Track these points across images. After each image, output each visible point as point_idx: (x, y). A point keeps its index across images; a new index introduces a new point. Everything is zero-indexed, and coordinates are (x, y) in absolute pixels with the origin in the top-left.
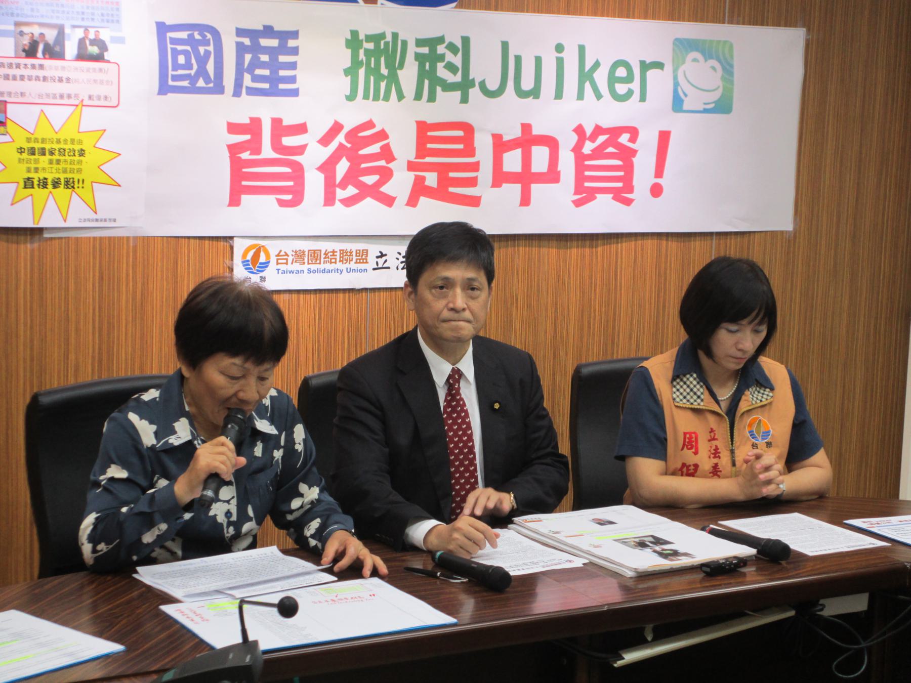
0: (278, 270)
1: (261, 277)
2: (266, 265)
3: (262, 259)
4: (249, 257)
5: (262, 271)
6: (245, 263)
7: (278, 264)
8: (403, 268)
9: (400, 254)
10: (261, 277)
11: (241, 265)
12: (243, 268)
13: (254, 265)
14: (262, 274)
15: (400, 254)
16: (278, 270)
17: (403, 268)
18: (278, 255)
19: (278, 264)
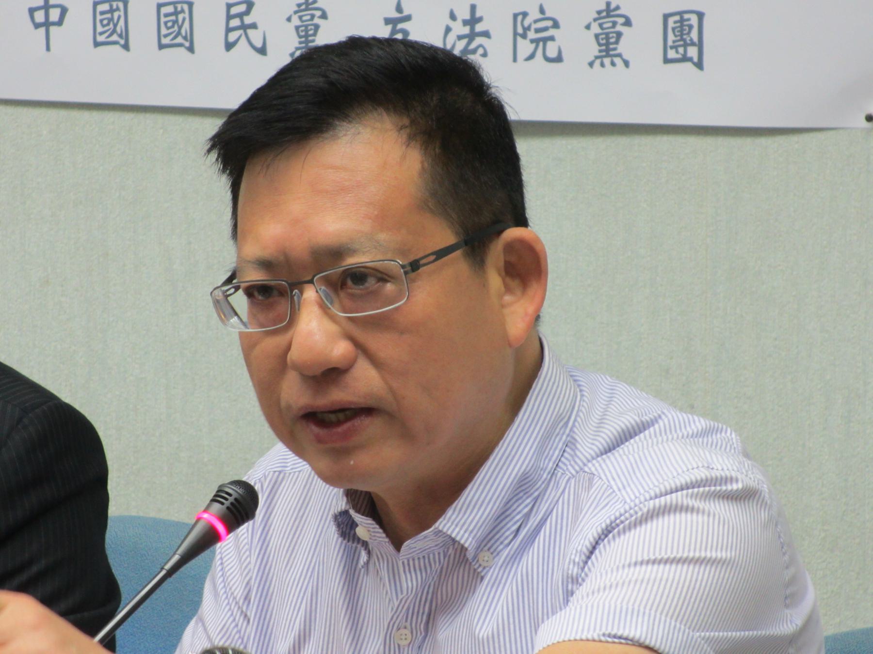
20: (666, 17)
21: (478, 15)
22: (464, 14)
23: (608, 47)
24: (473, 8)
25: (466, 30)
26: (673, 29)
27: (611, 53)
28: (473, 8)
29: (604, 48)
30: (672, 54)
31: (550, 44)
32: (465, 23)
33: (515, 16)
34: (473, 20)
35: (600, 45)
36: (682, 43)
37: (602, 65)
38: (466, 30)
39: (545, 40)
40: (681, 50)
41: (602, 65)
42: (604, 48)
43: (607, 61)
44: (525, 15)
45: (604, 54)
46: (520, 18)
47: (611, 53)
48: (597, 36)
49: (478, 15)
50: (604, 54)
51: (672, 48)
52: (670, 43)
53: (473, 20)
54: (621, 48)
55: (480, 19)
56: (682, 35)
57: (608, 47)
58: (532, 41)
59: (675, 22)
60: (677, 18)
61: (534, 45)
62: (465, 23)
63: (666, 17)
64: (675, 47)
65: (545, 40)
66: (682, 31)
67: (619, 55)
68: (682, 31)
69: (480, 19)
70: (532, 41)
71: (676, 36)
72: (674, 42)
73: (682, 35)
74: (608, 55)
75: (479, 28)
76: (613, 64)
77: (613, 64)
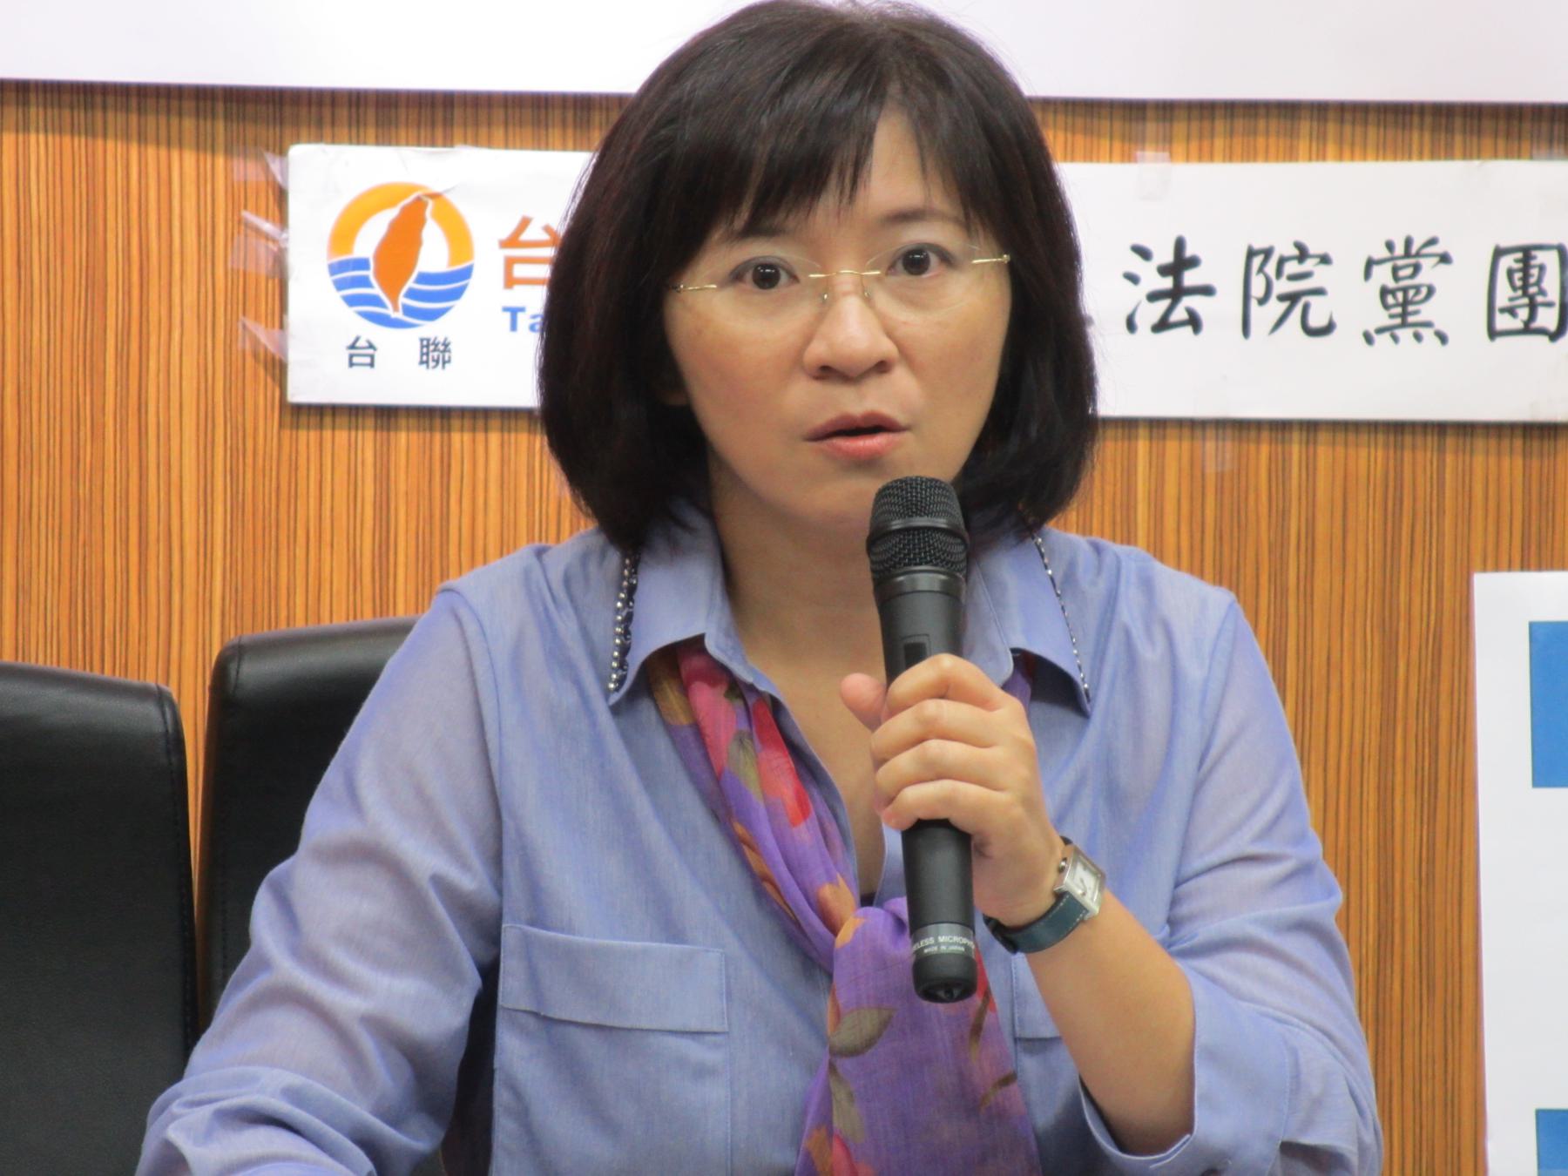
0: (514, 312)
1: (427, 346)
2: (451, 285)
3: (433, 255)
4: (367, 243)
5: (432, 315)
6: (346, 273)
7: (510, 281)
8: (1162, 325)
9: (1144, 253)
10: (427, 346)
11: (327, 281)
12: (336, 297)
13: (392, 285)
14: (429, 329)
15: (1144, 253)
16: (514, 312)
17: (1162, 325)
18: (512, 241)
19: (510, 281)
20: (1499, 253)
21: (1189, 252)
22: (1166, 256)
23: (1403, 305)
24: (1180, 245)
25: (1167, 283)
26: (1510, 273)
27: (1411, 319)
28: (1180, 245)
30: (1503, 322)
32: (1164, 271)
33: (1251, 254)
34: (1181, 263)
36: (1526, 301)
38: (1167, 283)
40: (1524, 313)
43: (1406, 334)
44: (1267, 253)
47: (1411, 319)
48: (1384, 292)
49: (1189, 252)
51: (1503, 310)
52: (1502, 299)
53: (1181, 263)
54: (1426, 312)
55: (1193, 262)
56: (1525, 287)
57: (1403, 305)
58: (1282, 298)
61: (1286, 305)
62: (1164, 271)
63: (1499, 253)
64: (1511, 311)
66: (1525, 278)
67: (1428, 324)
68: (1525, 278)
69: (1193, 262)
70: (1282, 298)
71: (1514, 288)
72: (1511, 299)
73: (1525, 287)
74: (1404, 325)
75: (1191, 278)
76: (1418, 337)
77: (1418, 337)
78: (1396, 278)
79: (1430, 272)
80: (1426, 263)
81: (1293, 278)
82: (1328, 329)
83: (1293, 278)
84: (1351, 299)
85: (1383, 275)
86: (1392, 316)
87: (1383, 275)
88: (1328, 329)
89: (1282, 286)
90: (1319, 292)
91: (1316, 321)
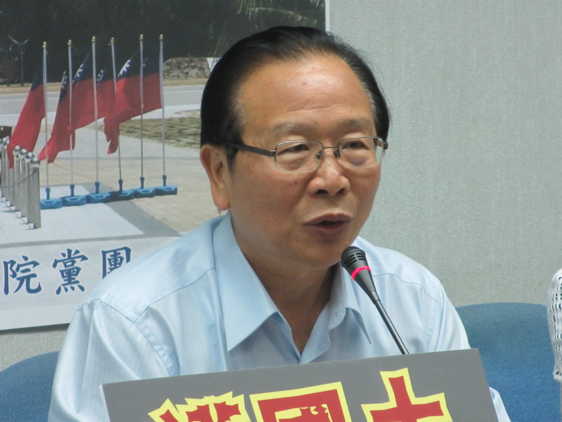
26: (110, 260)
27: (72, 281)
29: (67, 278)
31: (32, 280)
33: (6, 264)
35: (63, 277)
37: (66, 290)
39: (28, 278)
41: (66, 290)
42: (67, 278)
43: (68, 287)
44: (13, 263)
45: (67, 282)
46: (9, 265)
48: (62, 272)
50: (67, 282)
59: (111, 256)
60: (112, 253)
65: (28, 278)
68: (115, 261)
74: (70, 283)
78: (66, 266)
79: (79, 263)
80: (78, 260)
81: (23, 272)
82: (39, 289)
83: (23, 272)
84: (48, 276)
85: (61, 266)
86: (65, 280)
87: (61, 266)
88: (39, 289)
89: (19, 274)
90: (34, 276)
91: (33, 286)
